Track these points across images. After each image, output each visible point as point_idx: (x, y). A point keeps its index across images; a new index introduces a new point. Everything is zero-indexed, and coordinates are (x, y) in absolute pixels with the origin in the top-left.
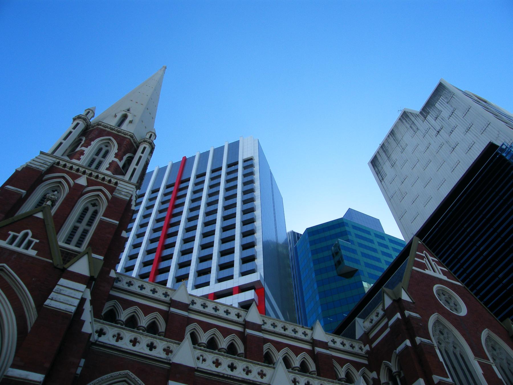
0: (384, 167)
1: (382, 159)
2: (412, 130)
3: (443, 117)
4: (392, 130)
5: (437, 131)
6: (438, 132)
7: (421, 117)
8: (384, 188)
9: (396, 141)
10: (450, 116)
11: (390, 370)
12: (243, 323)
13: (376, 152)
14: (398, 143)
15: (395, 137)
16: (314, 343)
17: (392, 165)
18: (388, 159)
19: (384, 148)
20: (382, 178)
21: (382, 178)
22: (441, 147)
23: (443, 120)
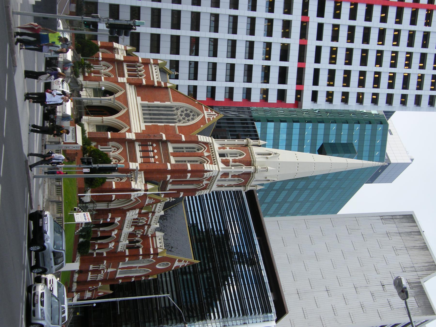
0: (394, 225)
3: (394, 297)
4: (428, 250)
6: (382, 286)
7: (415, 280)
9: (411, 248)
10: (389, 302)
11: (138, 242)
13: (418, 225)
14: (407, 248)
16: (149, 225)
19: (415, 234)
20: (384, 218)
21: (383, 219)
22: (368, 281)
23: (391, 295)
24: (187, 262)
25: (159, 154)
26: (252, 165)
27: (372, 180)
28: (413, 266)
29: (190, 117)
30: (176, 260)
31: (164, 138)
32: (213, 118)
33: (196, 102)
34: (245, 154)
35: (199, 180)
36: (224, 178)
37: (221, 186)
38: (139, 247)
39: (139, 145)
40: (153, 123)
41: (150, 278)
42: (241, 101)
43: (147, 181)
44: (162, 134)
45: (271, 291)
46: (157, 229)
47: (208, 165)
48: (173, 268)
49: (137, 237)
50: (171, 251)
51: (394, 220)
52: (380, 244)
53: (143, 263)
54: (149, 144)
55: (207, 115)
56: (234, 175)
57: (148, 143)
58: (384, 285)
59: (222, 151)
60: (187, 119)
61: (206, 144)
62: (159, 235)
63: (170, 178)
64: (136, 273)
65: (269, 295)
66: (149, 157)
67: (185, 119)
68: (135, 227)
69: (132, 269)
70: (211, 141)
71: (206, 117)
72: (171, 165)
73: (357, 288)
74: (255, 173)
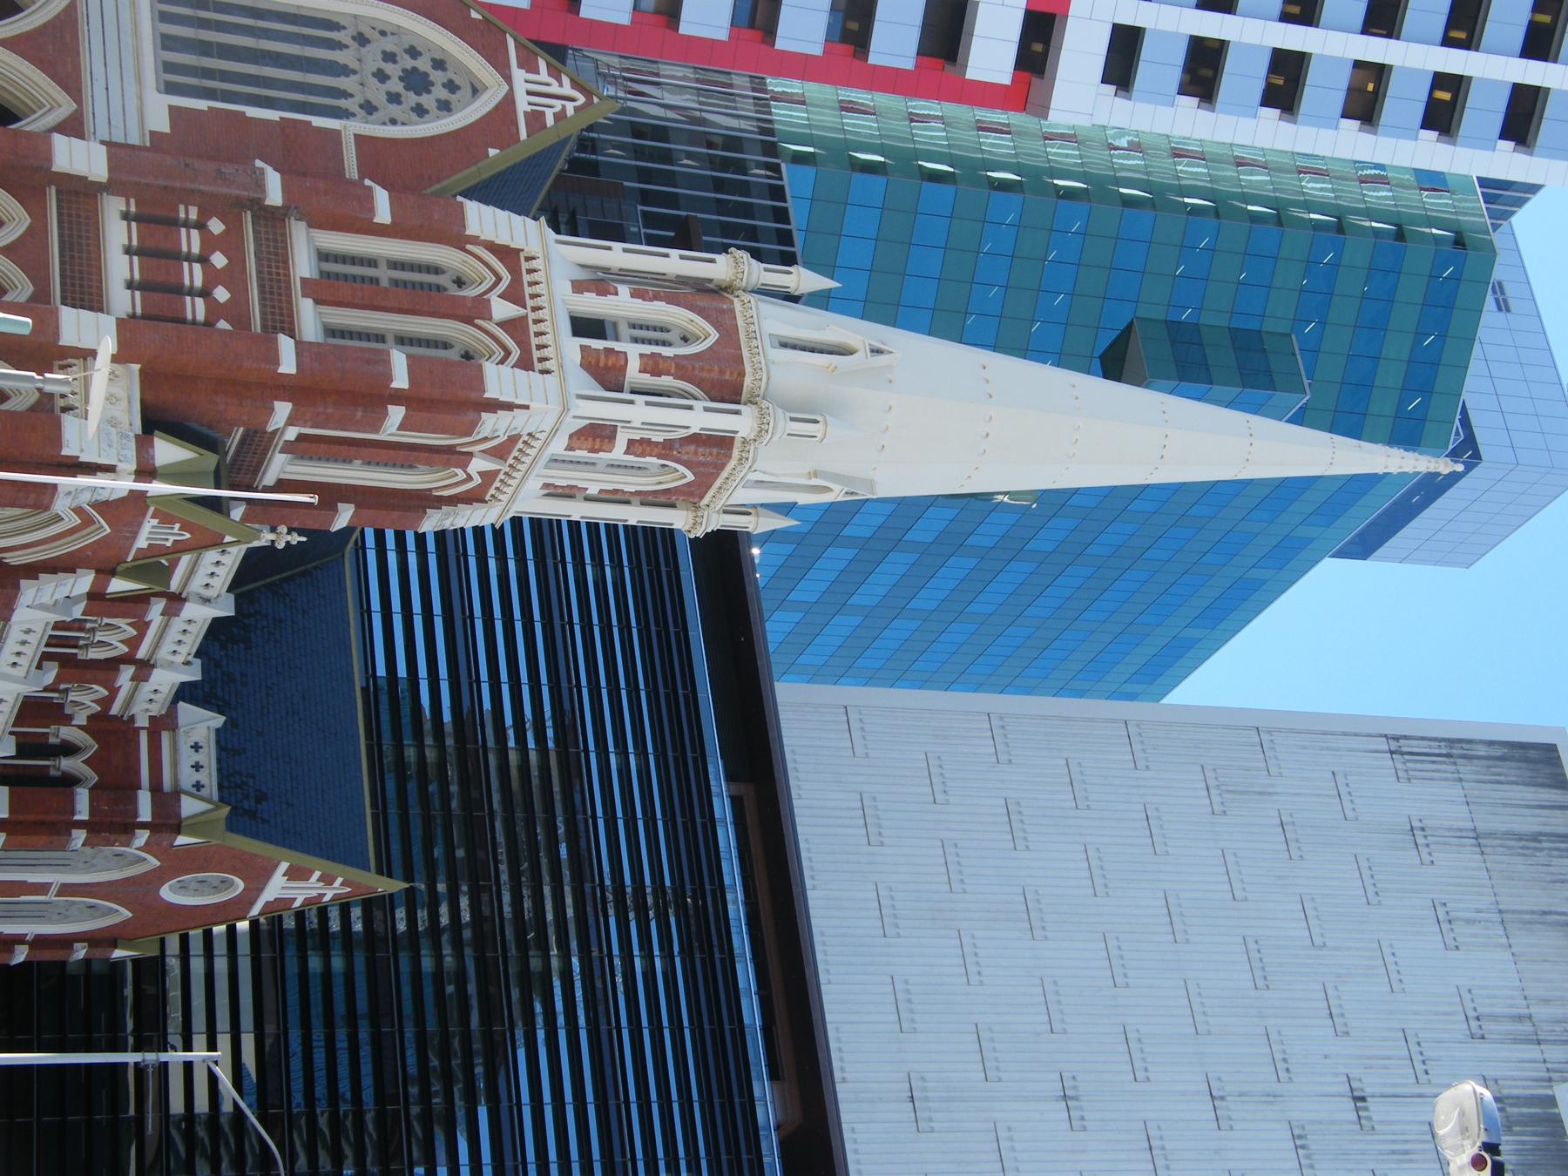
0: (1456, 792)
1: (1505, 805)
2: (1497, 1010)
3: (1411, 1161)
5: (1368, 1099)
7: (1525, 1088)
8: (1345, 734)
9: (1527, 917)
12: (184, 596)
14: (1507, 916)
15: (1557, 924)
16: (144, 668)
17: (1423, 829)
18: (1475, 830)
21: (1403, 754)
22: (1282, 1067)
23: (1394, 1152)
24: (340, 880)
25: (233, 277)
26: (744, 397)
27: (1363, 547)
28: (1526, 1011)
29: (429, 92)
30: (276, 866)
31: (274, 195)
32: (560, 116)
33: (474, 15)
34: (714, 335)
35: (450, 450)
36: (581, 454)
37: (568, 493)
38: (70, 781)
39: (126, 216)
40: (215, 99)
41: (118, 953)
42: (721, 33)
43: (155, 421)
44: (262, 171)
45: (774, 1075)
46: (185, 693)
47: (506, 370)
48: (255, 911)
49: (67, 720)
50: (252, 814)
51: (1455, 764)
52: (1368, 882)
53: (89, 866)
54: (182, 215)
55: (529, 93)
56: (643, 441)
57: (182, 208)
58: (1363, 1099)
59: (591, 305)
60: (411, 98)
61: (508, 255)
62: (201, 723)
63: (291, 421)
64: (40, 918)
65: (757, 1093)
66: (179, 290)
67: (399, 103)
68: (61, 667)
69: (23, 898)
70: (533, 248)
71: (523, 104)
72: (301, 347)
73: (1222, 1098)
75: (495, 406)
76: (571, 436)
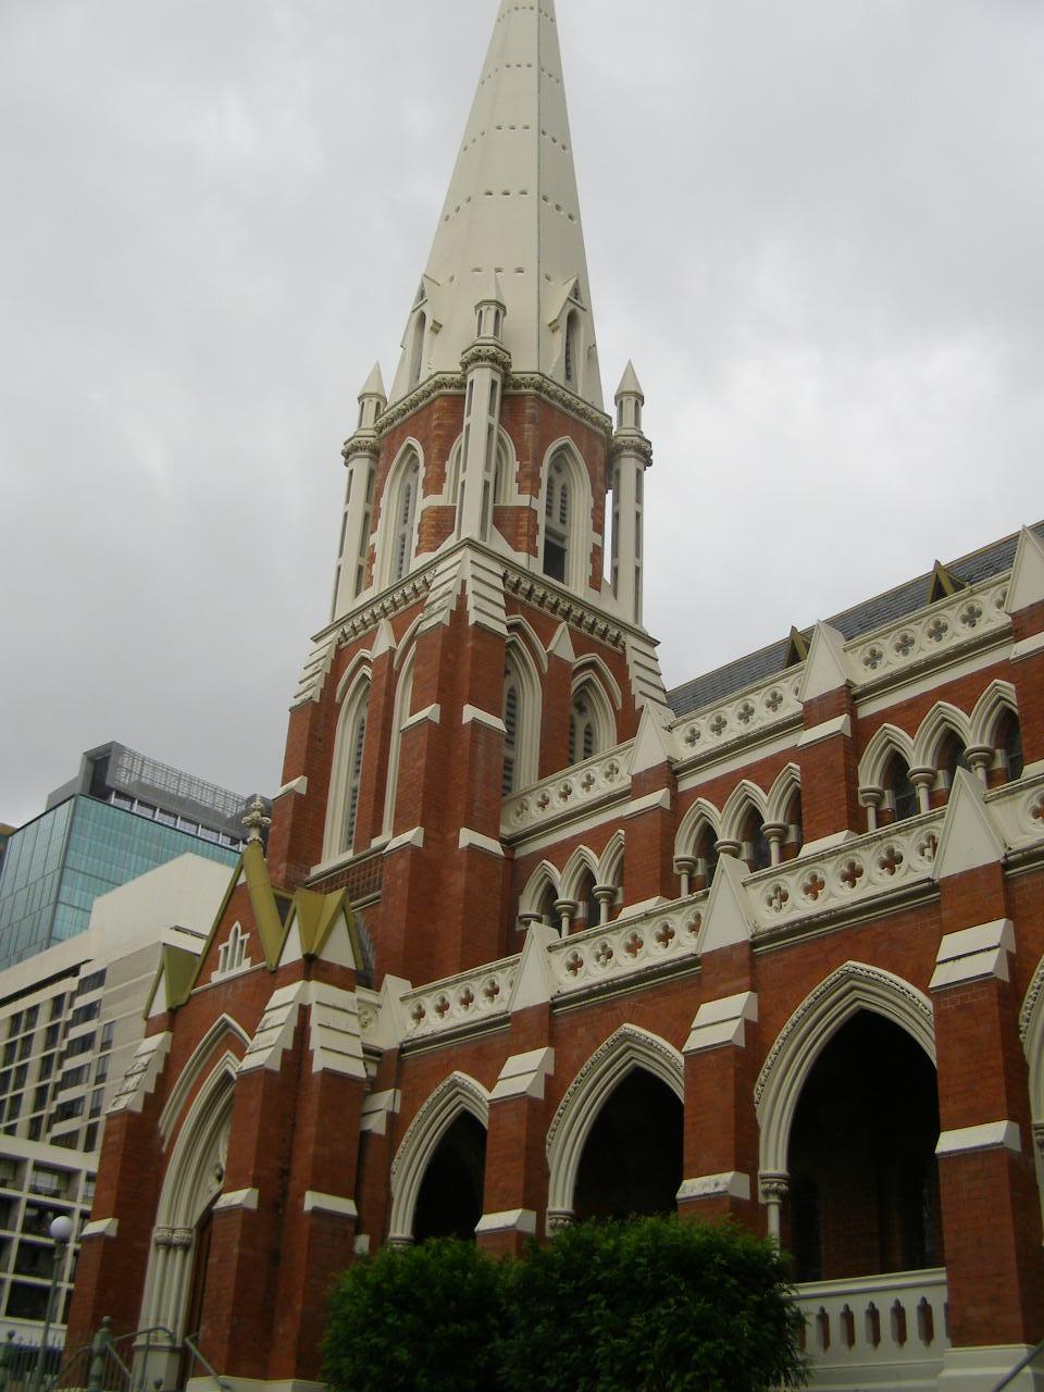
34: (411, 440)
74: (506, 366)
75: (459, 614)
76: (516, 551)
